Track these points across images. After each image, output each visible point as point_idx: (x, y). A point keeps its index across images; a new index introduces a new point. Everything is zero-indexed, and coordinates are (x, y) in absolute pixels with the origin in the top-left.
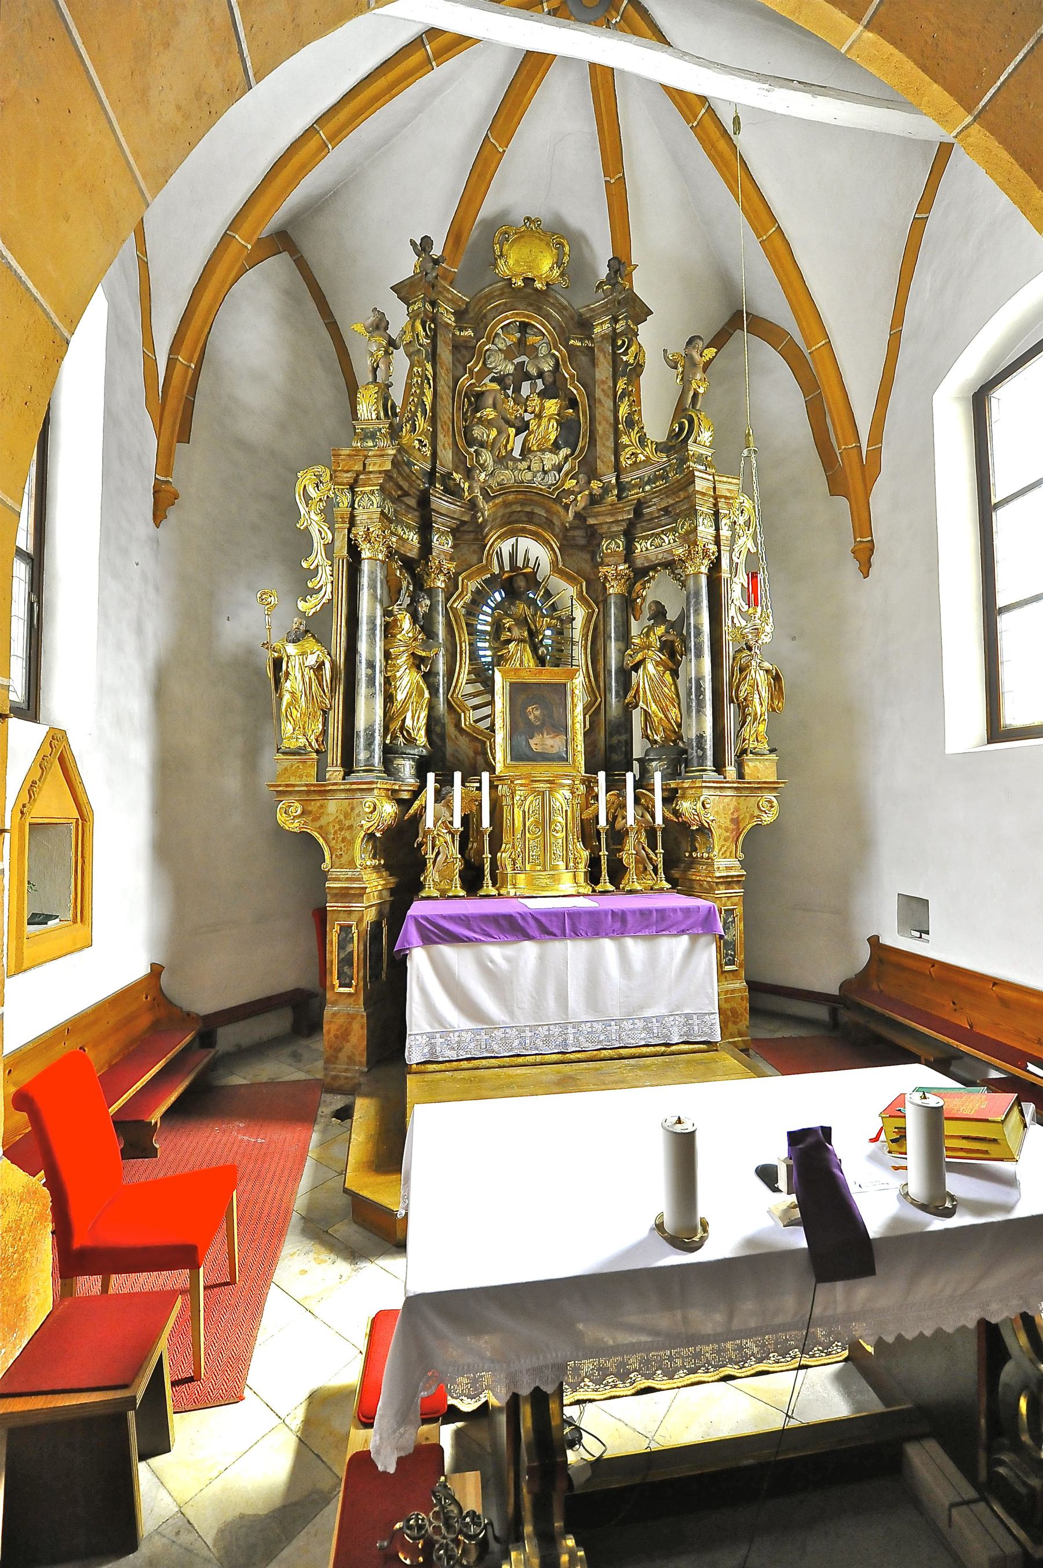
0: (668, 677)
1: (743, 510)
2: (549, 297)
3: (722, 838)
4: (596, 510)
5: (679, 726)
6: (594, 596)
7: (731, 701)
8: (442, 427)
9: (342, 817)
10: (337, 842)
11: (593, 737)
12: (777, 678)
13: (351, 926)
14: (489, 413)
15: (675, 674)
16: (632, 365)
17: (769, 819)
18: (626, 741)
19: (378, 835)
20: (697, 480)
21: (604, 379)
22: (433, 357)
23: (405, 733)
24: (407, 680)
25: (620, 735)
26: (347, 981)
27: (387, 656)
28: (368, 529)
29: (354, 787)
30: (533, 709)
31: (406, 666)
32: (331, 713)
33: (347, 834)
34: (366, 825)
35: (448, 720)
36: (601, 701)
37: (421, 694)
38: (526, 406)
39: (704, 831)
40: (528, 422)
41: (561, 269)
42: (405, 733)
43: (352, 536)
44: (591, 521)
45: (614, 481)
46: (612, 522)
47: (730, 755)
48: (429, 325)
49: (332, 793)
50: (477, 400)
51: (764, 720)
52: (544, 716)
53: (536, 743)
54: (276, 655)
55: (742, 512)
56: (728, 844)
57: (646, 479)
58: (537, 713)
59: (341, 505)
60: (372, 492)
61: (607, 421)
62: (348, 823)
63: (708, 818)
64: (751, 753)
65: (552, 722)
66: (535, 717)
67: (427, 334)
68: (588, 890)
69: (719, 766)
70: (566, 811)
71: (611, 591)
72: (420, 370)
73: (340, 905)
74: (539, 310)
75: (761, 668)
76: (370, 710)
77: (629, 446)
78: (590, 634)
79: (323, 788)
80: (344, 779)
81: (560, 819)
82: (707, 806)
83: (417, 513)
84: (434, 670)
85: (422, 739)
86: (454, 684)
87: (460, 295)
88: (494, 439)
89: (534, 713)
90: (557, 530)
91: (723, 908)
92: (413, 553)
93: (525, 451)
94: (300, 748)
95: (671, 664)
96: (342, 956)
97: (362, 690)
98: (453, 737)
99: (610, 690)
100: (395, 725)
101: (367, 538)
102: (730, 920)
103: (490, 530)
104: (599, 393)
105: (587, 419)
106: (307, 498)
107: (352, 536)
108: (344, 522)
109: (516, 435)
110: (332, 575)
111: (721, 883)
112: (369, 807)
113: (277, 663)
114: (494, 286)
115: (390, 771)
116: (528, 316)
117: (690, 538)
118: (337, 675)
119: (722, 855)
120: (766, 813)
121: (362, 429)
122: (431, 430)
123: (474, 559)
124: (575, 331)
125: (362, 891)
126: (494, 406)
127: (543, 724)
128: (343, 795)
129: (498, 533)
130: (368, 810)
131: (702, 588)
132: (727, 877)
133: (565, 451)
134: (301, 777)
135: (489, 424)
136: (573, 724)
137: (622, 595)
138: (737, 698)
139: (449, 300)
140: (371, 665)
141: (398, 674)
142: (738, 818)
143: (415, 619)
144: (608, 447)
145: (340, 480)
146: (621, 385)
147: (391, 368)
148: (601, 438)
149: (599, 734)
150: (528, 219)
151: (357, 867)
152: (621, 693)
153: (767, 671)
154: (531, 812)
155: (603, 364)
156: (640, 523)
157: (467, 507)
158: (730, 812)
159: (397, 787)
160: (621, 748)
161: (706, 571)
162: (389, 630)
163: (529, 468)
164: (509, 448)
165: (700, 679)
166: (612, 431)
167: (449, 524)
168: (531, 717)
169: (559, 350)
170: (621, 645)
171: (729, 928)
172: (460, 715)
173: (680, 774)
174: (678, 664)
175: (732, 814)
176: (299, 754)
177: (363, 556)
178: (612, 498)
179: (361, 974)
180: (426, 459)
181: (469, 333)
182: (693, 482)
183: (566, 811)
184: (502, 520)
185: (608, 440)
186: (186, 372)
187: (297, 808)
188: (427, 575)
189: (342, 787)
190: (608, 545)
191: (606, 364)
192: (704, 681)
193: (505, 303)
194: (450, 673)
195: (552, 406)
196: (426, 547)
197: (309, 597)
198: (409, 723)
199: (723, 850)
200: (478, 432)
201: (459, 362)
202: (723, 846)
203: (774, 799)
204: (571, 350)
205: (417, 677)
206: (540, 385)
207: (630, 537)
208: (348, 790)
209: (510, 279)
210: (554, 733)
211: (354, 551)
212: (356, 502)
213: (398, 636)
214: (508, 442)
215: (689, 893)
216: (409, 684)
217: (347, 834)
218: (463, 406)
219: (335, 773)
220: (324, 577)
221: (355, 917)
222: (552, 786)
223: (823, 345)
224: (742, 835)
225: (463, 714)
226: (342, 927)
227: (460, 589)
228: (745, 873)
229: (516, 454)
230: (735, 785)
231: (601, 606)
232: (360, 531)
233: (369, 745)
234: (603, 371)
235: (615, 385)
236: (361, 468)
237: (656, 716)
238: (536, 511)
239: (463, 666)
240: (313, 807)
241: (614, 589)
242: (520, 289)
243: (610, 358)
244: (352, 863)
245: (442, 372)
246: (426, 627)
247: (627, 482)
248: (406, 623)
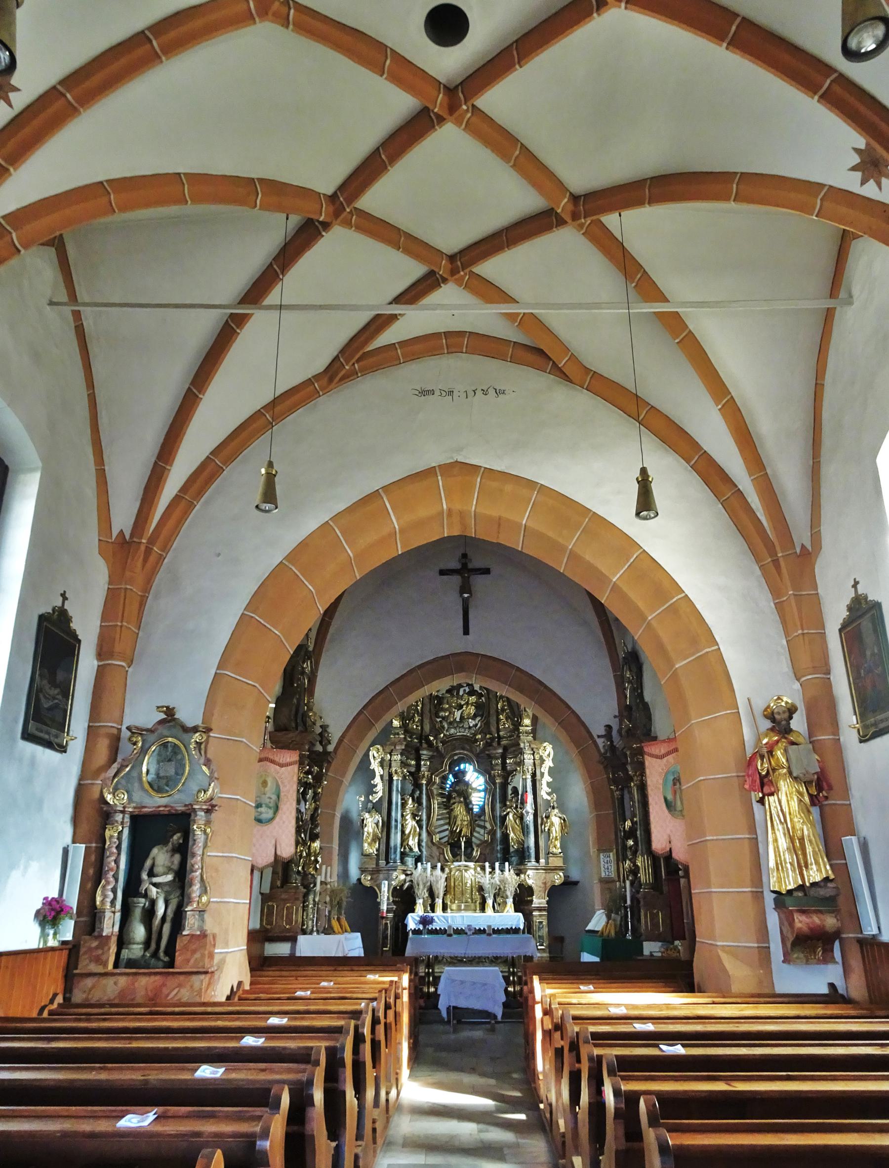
7: (542, 832)
24: (410, 823)
27: (402, 816)
44: (487, 752)
76: (396, 838)
85: (416, 849)
92: (413, 770)
93: (462, 718)
97: (393, 830)
100: (405, 843)
101: (396, 772)
106: (374, 757)
133: (478, 719)
135: (445, 710)
140: (396, 821)
153: (560, 818)
162: (404, 805)
178: (495, 744)
195: (473, 699)
196: (418, 766)
205: (414, 823)
206: (467, 690)
207: (504, 758)
211: (391, 776)
219: (382, 862)
229: (458, 719)
232: (393, 769)
233: (395, 852)
240: (375, 876)
246: (418, 801)
248: (410, 801)
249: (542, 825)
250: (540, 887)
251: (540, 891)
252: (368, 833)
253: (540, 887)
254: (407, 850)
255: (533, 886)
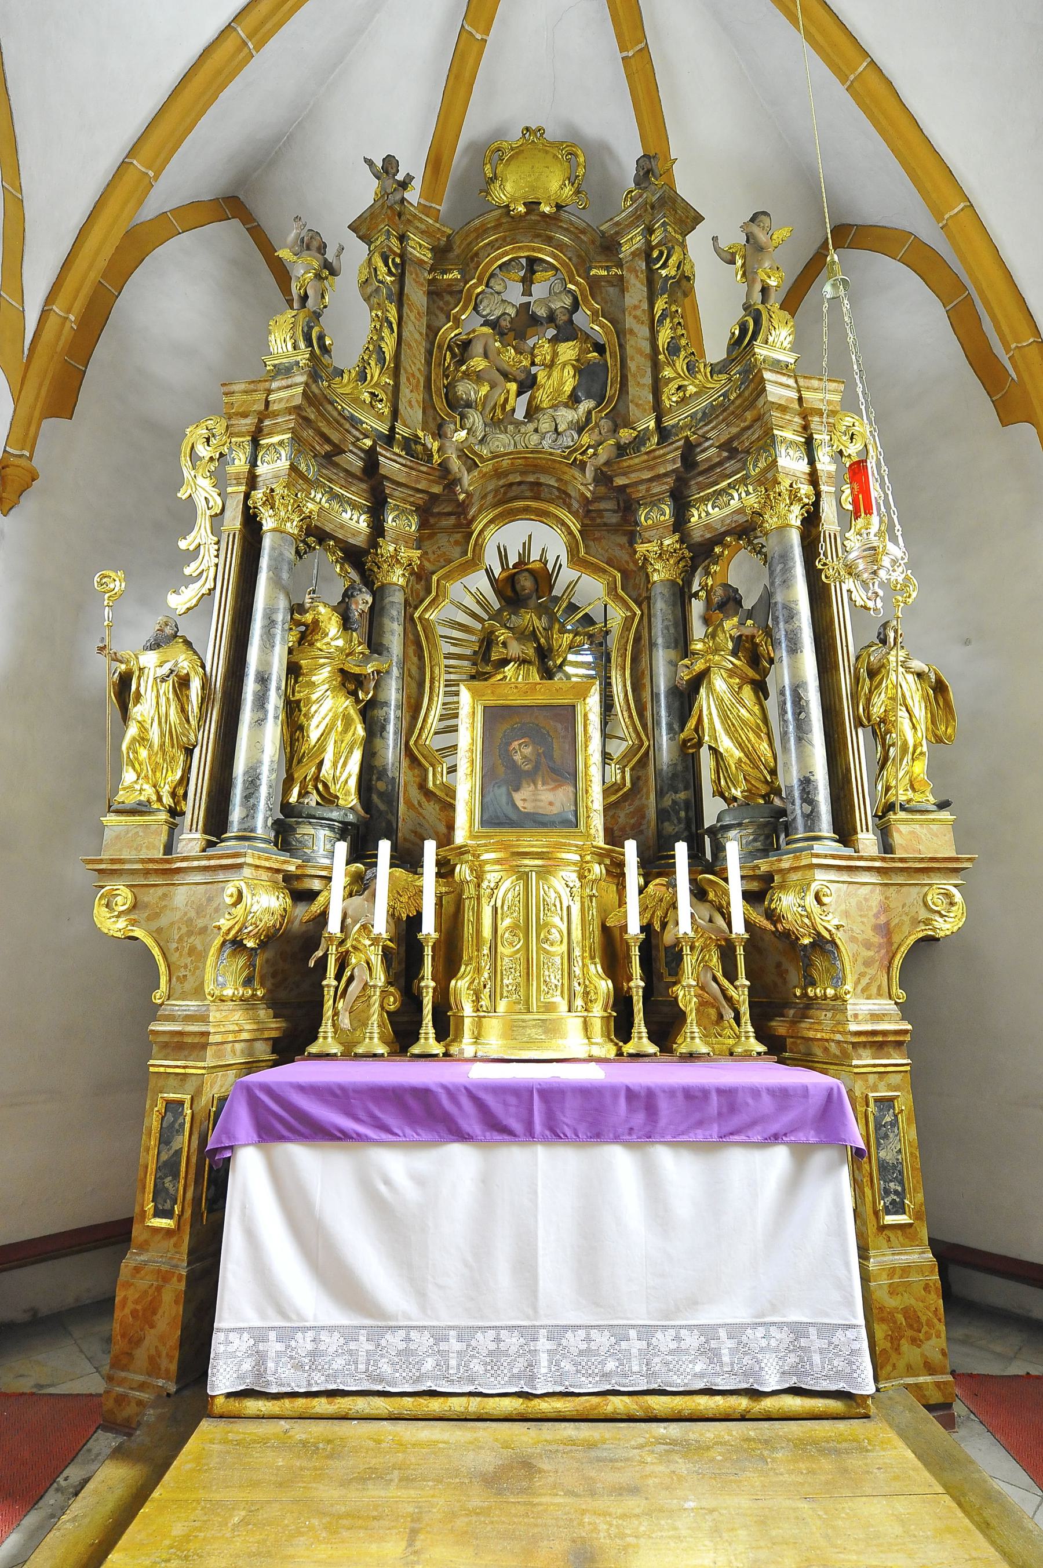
0: (747, 692)
1: (853, 434)
2: (561, 221)
3: (860, 960)
4: (625, 464)
5: (773, 772)
6: (634, 594)
7: (859, 723)
8: (408, 379)
9: (192, 914)
10: (181, 955)
11: (637, 803)
12: (940, 688)
13: (181, 1103)
14: (478, 363)
15: (760, 688)
16: (674, 278)
17: (948, 926)
18: (687, 803)
19: (250, 944)
20: (769, 387)
21: (637, 303)
22: (400, 299)
23: (320, 786)
25: (676, 793)
26: (167, 1206)
27: (293, 670)
28: (272, 490)
29: (213, 863)
30: (520, 745)
31: (327, 686)
32: (197, 751)
33: (197, 941)
34: (225, 923)
35: (405, 777)
36: (649, 746)
37: (348, 722)
38: (533, 356)
39: (824, 945)
40: (535, 377)
41: (576, 185)
42: (320, 786)
43: (250, 503)
44: (620, 481)
45: (652, 424)
46: (651, 480)
47: (864, 812)
48: (393, 260)
49: (182, 875)
50: (463, 348)
51: (921, 753)
52: (539, 755)
53: (525, 799)
54: (123, 667)
55: (852, 439)
56: (871, 971)
57: (700, 415)
58: (528, 751)
59: (237, 462)
60: (281, 443)
61: (640, 352)
62: (200, 923)
63: (829, 922)
64: (903, 808)
65: (551, 764)
66: (524, 757)
67: (389, 270)
68: (609, 1051)
69: (844, 832)
70: (568, 907)
71: (656, 577)
72: (380, 313)
73: (179, 1063)
74: (549, 240)
75: (908, 669)
76: (256, 746)
77: (674, 379)
78: (630, 648)
79: (167, 866)
80: (204, 850)
81: (556, 920)
82: (825, 900)
83: (364, 486)
84: (382, 697)
86: (419, 725)
87: (438, 225)
88: (486, 396)
89: (522, 752)
90: (575, 505)
91: (871, 1095)
92: (359, 541)
93: (532, 411)
94: (140, 803)
95: (751, 673)
96: (164, 1157)
98: (416, 803)
99: (659, 724)
101: (270, 501)
102: (888, 1119)
103: (479, 511)
104: (630, 322)
105: (616, 361)
107: (250, 503)
108: (239, 484)
109: (519, 393)
110: (217, 556)
111: (864, 1045)
112: (232, 896)
113: (125, 681)
114: (487, 216)
115: (290, 844)
116: (534, 250)
117: (768, 479)
118: (209, 695)
119: (863, 991)
120: (942, 916)
121: (275, 366)
122: (392, 383)
123: (458, 550)
124: (599, 258)
125: (203, 1040)
126: (486, 356)
127: (537, 768)
128: (198, 878)
129: (491, 516)
130: (229, 901)
131: (792, 547)
132: (874, 1033)
133: (586, 405)
134: (138, 849)
135: (478, 377)
136: (586, 767)
137: (673, 583)
138: (869, 720)
139: (422, 232)
140: (263, 680)
141: (314, 697)
142: (887, 924)
143: (346, 623)
144: (644, 385)
145: (236, 430)
146: (660, 305)
147: (327, 297)
148: (634, 376)
149: (648, 798)
150: (527, 129)
151: (206, 999)
152: (676, 727)
153: (920, 675)
154: (506, 908)
155: (634, 285)
156: (694, 477)
157: (437, 473)
158: (871, 914)
159: (292, 868)
160: (677, 813)
161: (799, 523)
163: (536, 430)
164: (508, 408)
165: (798, 686)
166: (649, 364)
167: (412, 499)
168: (517, 758)
169: (576, 284)
170: (672, 654)
171: (886, 1137)
172: (426, 770)
173: (778, 848)
174: (765, 673)
175: (876, 916)
176: (141, 813)
177: (264, 528)
179: (190, 1195)
180: (383, 419)
181: (455, 275)
182: (764, 390)
183: (568, 907)
184: (494, 497)
185: (643, 376)
186: (63, 324)
187: (124, 897)
188: (379, 568)
189: (196, 864)
190: (648, 513)
191: (638, 285)
192: (806, 690)
193: (504, 239)
194: (413, 708)
195: (568, 351)
196: (377, 529)
197: (183, 588)
198: (327, 771)
199: (864, 981)
200: (465, 389)
201: (441, 310)
202: (862, 975)
203: (954, 891)
204: (594, 284)
205: (345, 703)
208: (206, 869)
209: (508, 206)
210: (554, 781)
211: (252, 525)
212: (259, 458)
213: (318, 645)
214: (506, 400)
215: (806, 1062)
216: (331, 714)
217: (197, 941)
218: (445, 360)
220: (208, 559)
221: (191, 1085)
222: (550, 862)
223: (962, 210)
224: (898, 956)
225: (431, 769)
226: (169, 1103)
227: (434, 593)
228: (909, 1027)
229: (520, 415)
230: (877, 864)
231: (645, 606)
234: (636, 293)
235: (652, 305)
236: (263, 407)
237: (732, 756)
238: (542, 480)
239: (436, 699)
240: (151, 896)
241: (660, 573)
242: (521, 217)
243: (643, 276)
244: (198, 992)
245: (410, 316)
247: (673, 426)
248: (332, 626)
249: (855, 697)
250: (868, 945)
251: (867, 963)
252: (143, 728)
253: (868, 945)
254: (313, 799)
255: (840, 937)
